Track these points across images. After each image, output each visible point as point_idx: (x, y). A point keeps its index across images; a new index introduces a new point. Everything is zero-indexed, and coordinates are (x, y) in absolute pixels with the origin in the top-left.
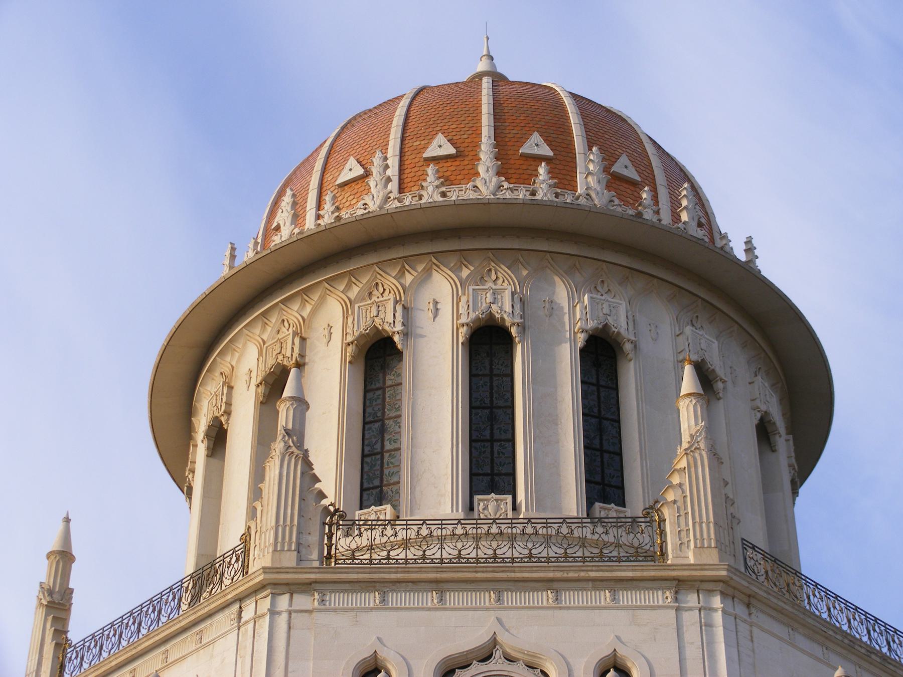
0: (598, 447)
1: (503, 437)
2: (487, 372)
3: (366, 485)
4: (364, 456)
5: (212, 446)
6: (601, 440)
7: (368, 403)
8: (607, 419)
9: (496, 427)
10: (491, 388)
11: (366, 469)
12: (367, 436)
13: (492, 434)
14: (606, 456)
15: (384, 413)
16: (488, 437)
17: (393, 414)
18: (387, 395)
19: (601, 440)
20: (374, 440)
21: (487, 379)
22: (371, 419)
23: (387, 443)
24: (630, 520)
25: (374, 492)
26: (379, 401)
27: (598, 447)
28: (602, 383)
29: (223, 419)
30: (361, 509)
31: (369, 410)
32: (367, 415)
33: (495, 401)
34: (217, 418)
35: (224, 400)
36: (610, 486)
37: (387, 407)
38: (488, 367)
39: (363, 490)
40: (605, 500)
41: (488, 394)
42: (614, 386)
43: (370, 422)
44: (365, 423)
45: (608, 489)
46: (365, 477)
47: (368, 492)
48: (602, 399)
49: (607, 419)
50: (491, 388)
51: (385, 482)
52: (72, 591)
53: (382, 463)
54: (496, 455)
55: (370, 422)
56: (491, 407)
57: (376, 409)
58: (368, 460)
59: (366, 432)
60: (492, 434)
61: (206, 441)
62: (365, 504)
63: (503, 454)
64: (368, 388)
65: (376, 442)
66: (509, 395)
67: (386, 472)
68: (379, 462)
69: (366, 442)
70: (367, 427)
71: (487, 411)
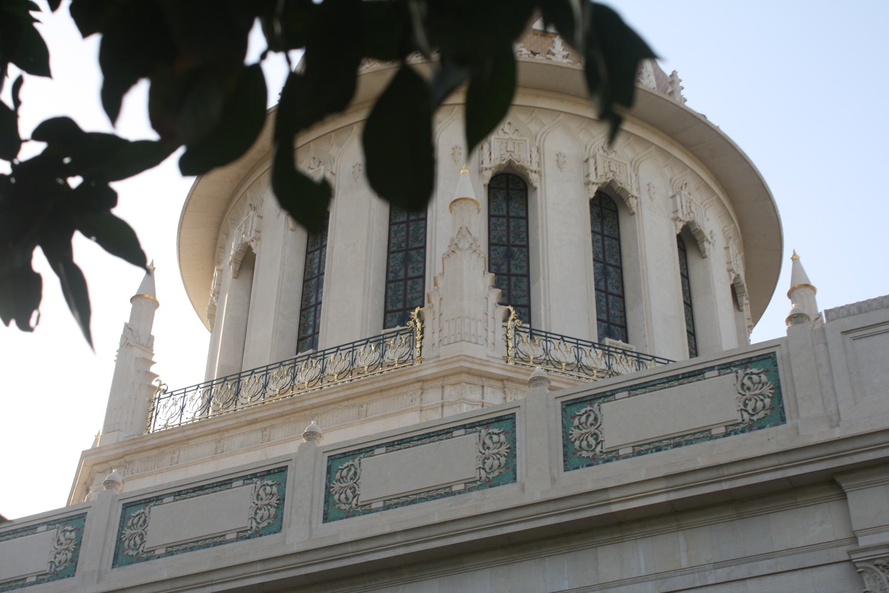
0: (604, 289)
1: (519, 272)
2: (505, 213)
3: (390, 308)
4: (388, 282)
5: (237, 269)
6: (606, 282)
7: (393, 235)
8: (611, 265)
9: (513, 262)
10: (508, 227)
11: (390, 293)
12: (392, 264)
13: (509, 269)
14: (611, 297)
15: (407, 244)
16: (505, 271)
17: (416, 245)
18: (411, 228)
19: (606, 282)
20: (398, 268)
21: (505, 220)
22: (394, 249)
23: (410, 271)
24: (635, 355)
25: (398, 314)
26: (403, 233)
27: (604, 289)
28: (606, 233)
29: (253, 245)
30: (384, 328)
31: (394, 241)
32: (391, 245)
33: (512, 240)
34: (246, 243)
35: (254, 227)
36: (615, 325)
37: (411, 238)
38: (505, 210)
39: (386, 312)
40: (611, 335)
41: (505, 233)
42: (617, 236)
43: (394, 252)
44: (389, 252)
45: (612, 327)
46: (389, 300)
47: (393, 314)
48: (606, 247)
49: (611, 265)
50: (508, 227)
51: (408, 306)
52: (255, 255)
53: (405, 289)
54: (513, 287)
55: (394, 252)
56: (509, 245)
57: (400, 240)
58: (392, 285)
59: (391, 261)
60: (509, 269)
61: (233, 264)
62: (388, 324)
63: (520, 287)
64: (394, 221)
65: (400, 270)
66: (524, 235)
67: (409, 297)
68: (402, 288)
69: (391, 270)
70: (391, 256)
71: (502, 249)
